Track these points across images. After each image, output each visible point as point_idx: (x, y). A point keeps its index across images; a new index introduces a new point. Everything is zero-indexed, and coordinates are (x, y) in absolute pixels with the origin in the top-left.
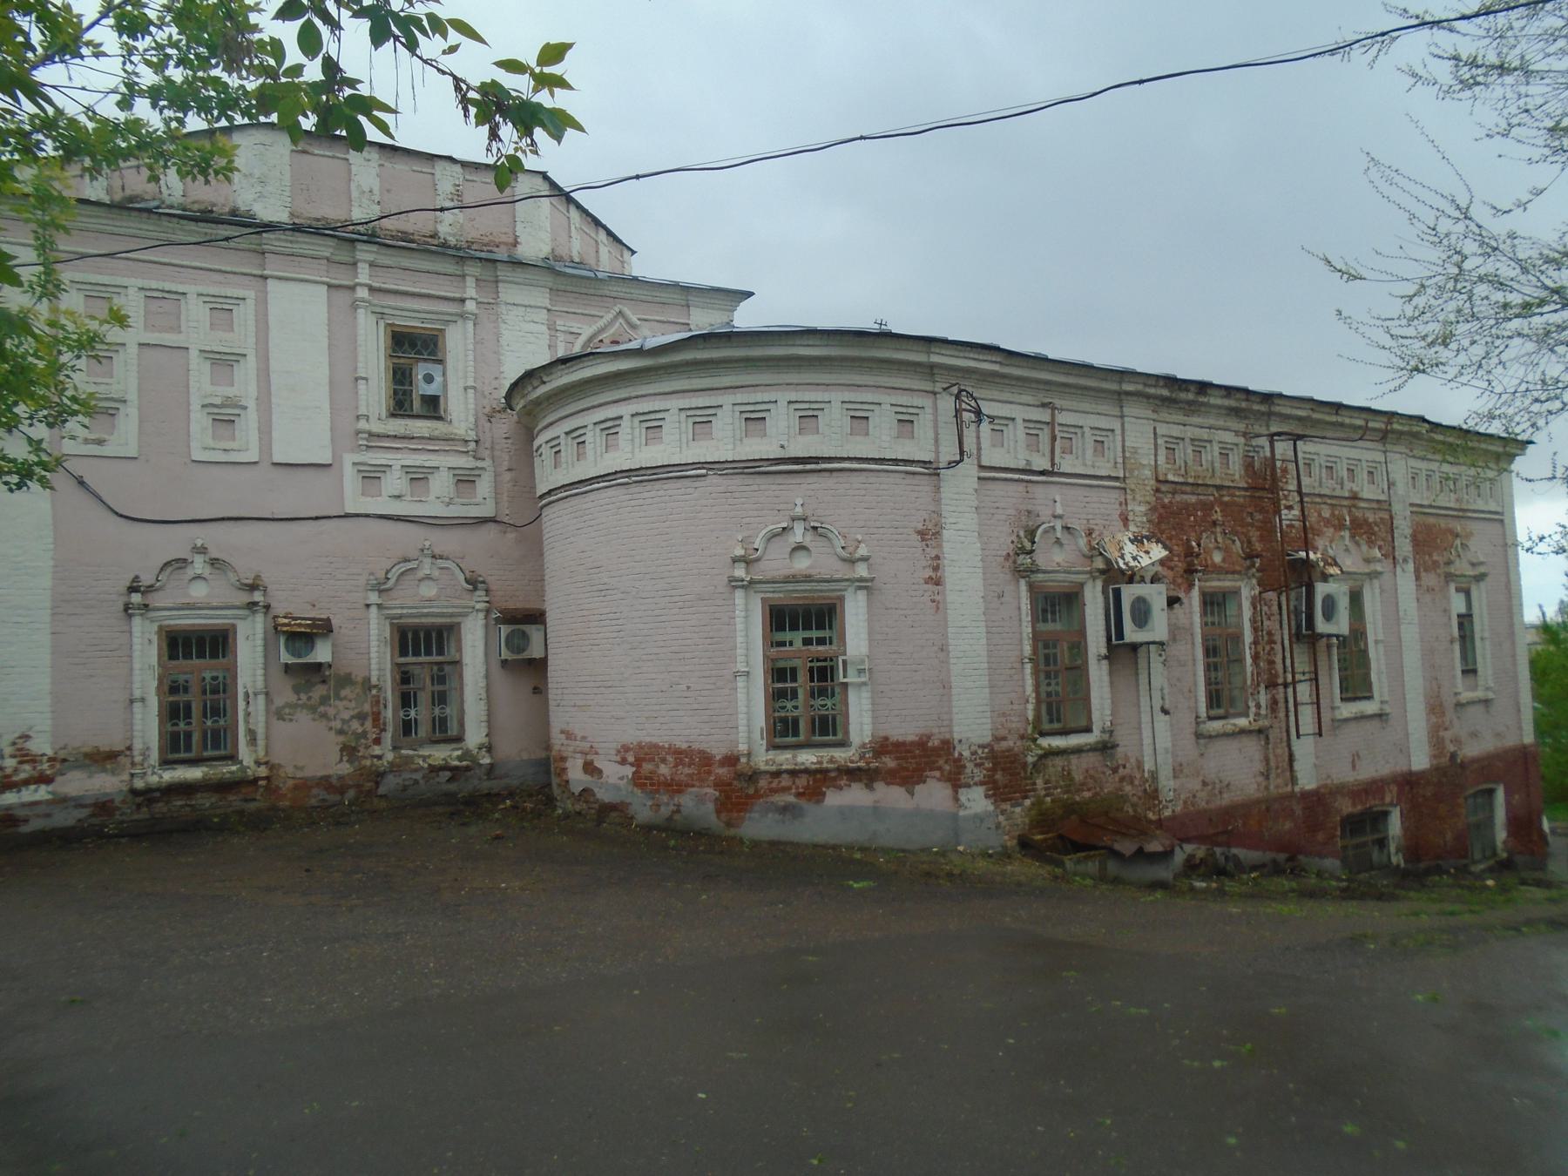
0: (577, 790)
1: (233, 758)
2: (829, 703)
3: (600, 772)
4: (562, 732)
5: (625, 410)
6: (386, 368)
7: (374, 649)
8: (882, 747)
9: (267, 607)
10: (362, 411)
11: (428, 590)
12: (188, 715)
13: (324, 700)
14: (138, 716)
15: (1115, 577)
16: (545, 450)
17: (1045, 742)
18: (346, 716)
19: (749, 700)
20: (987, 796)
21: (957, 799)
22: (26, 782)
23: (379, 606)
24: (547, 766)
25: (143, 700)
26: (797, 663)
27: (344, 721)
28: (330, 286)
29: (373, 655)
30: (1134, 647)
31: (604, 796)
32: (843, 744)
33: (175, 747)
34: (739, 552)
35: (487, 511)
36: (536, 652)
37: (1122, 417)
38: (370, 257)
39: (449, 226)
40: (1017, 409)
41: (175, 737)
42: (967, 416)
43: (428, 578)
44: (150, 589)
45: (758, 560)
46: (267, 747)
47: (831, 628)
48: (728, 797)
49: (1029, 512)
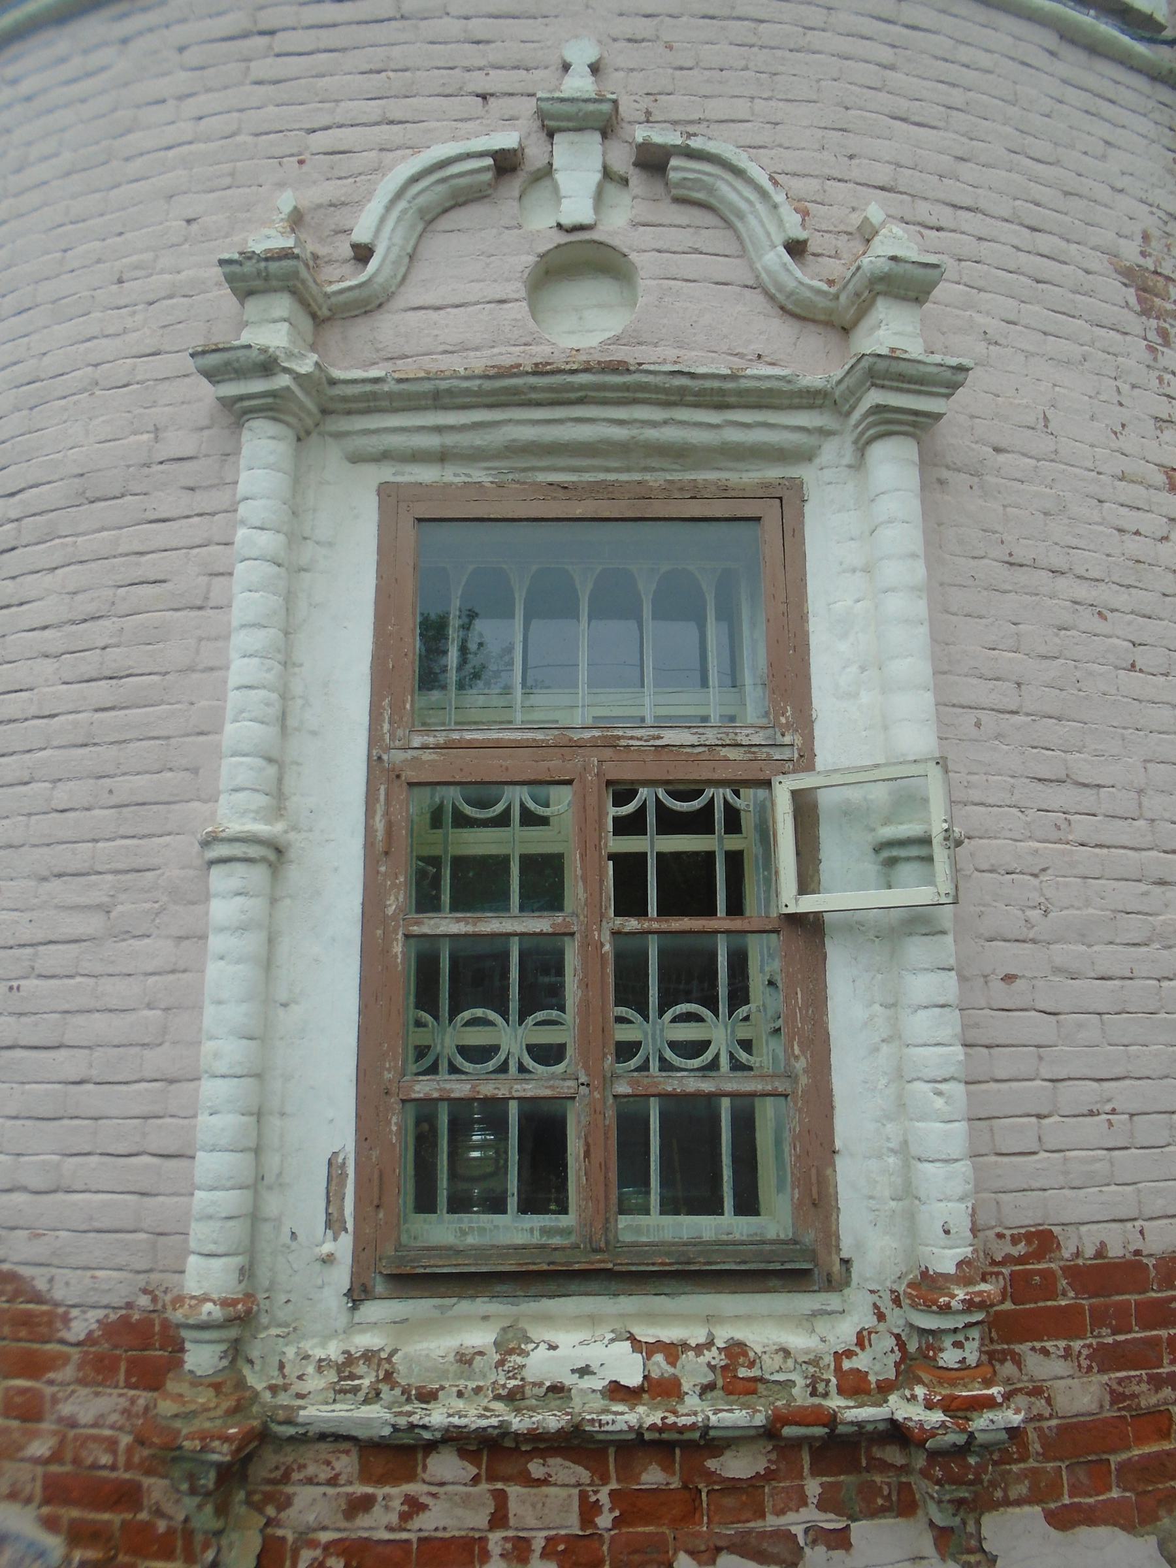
2: (718, 1032)
8: (1034, 1289)
32: (801, 1269)
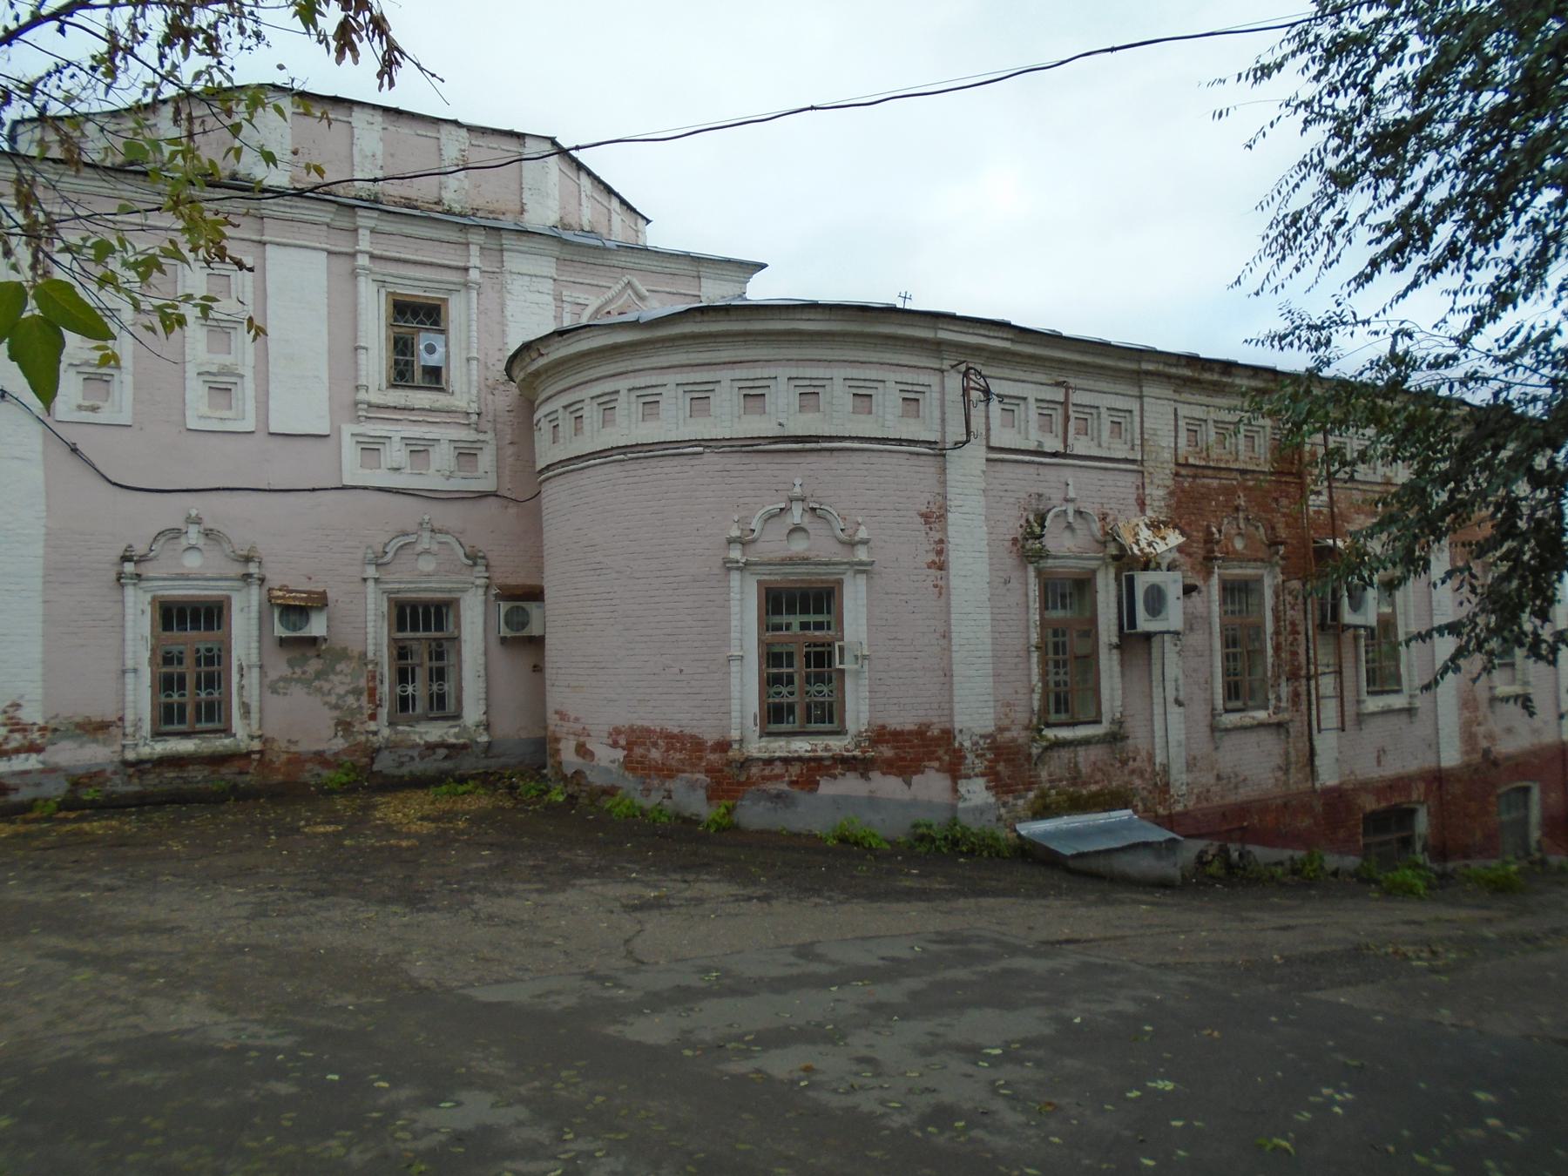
0: (569, 772)
1: (227, 731)
3: (592, 754)
4: (556, 712)
5: (622, 384)
6: (387, 338)
7: (370, 624)
8: (880, 735)
9: (262, 580)
10: (362, 381)
11: (427, 565)
12: (182, 686)
13: (319, 675)
14: (130, 687)
15: (1127, 563)
16: (544, 424)
17: (1050, 734)
18: (341, 690)
19: (742, 685)
20: (988, 788)
21: (956, 791)
22: (17, 751)
23: (377, 580)
24: (542, 746)
25: (135, 671)
26: (793, 648)
27: (340, 697)
28: (330, 253)
29: (370, 630)
30: (1148, 637)
31: (596, 779)
32: (841, 732)
33: (168, 718)
34: (735, 533)
35: (488, 485)
36: (534, 629)
37: (1141, 397)
38: (372, 223)
39: (455, 191)
40: (1032, 389)
41: (168, 708)
42: (975, 395)
43: (427, 552)
44: (142, 559)
45: (753, 541)
46: (261, 720)
47: (829, 612)
48: (719, 783)
49: (1040, 495)
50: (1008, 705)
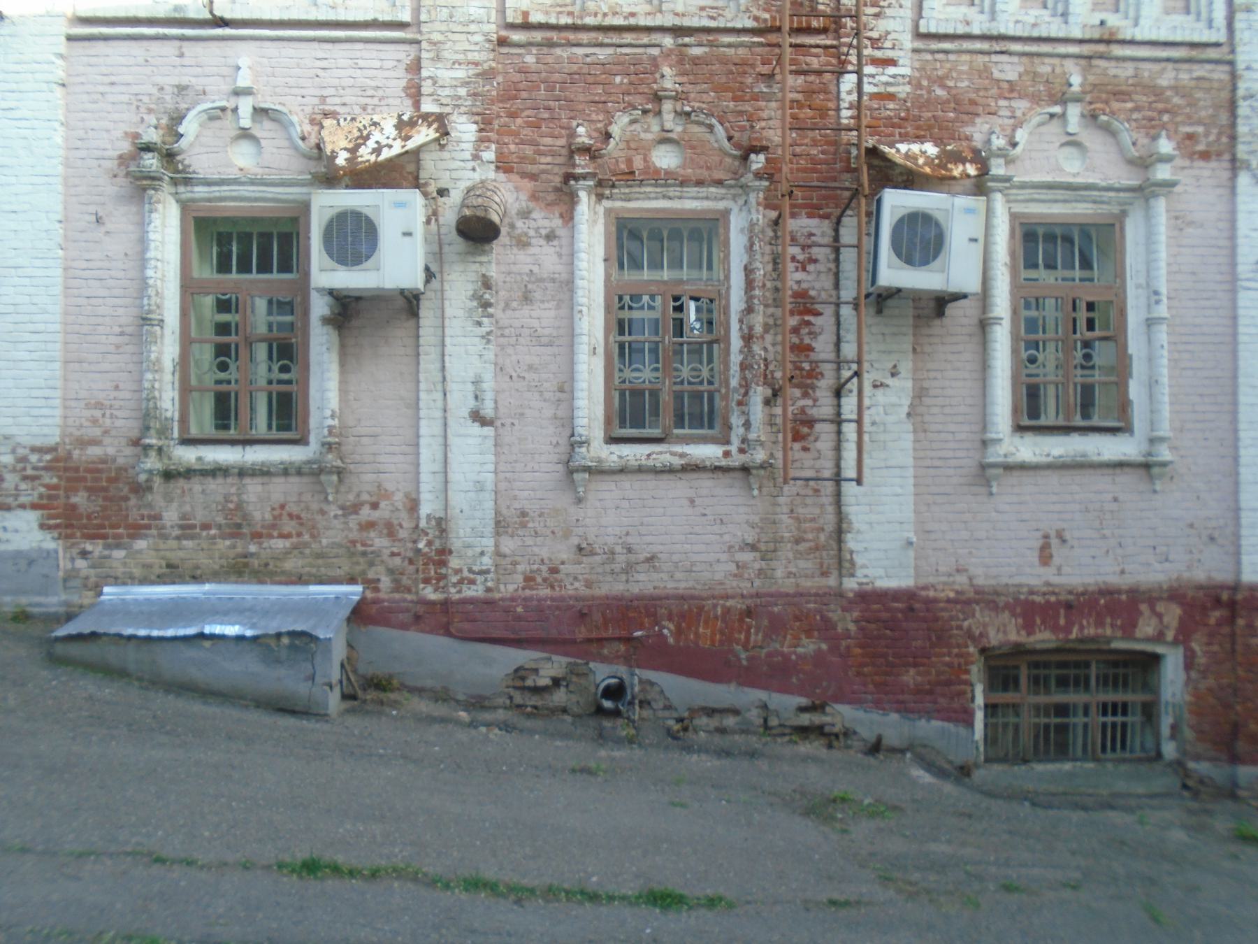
20: (42, 526)
50: (99, 405)
